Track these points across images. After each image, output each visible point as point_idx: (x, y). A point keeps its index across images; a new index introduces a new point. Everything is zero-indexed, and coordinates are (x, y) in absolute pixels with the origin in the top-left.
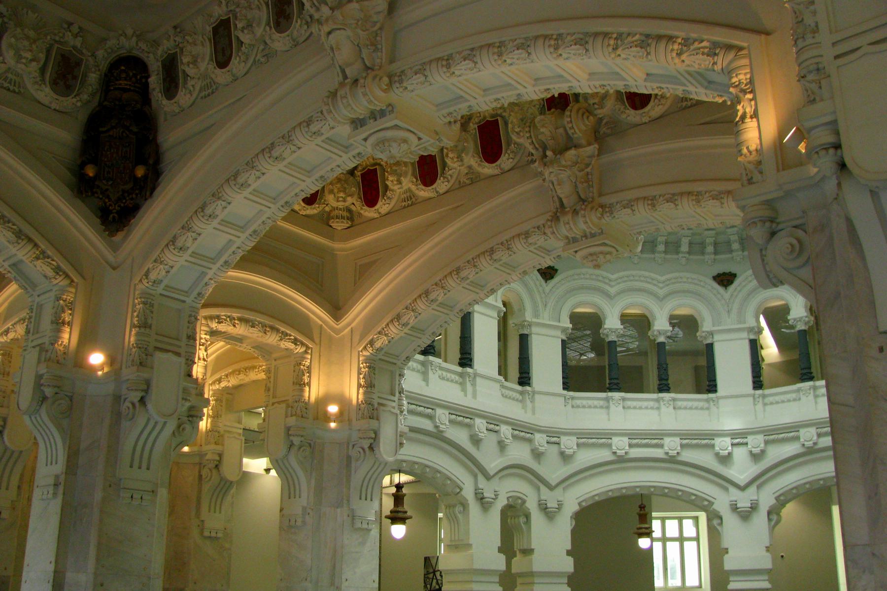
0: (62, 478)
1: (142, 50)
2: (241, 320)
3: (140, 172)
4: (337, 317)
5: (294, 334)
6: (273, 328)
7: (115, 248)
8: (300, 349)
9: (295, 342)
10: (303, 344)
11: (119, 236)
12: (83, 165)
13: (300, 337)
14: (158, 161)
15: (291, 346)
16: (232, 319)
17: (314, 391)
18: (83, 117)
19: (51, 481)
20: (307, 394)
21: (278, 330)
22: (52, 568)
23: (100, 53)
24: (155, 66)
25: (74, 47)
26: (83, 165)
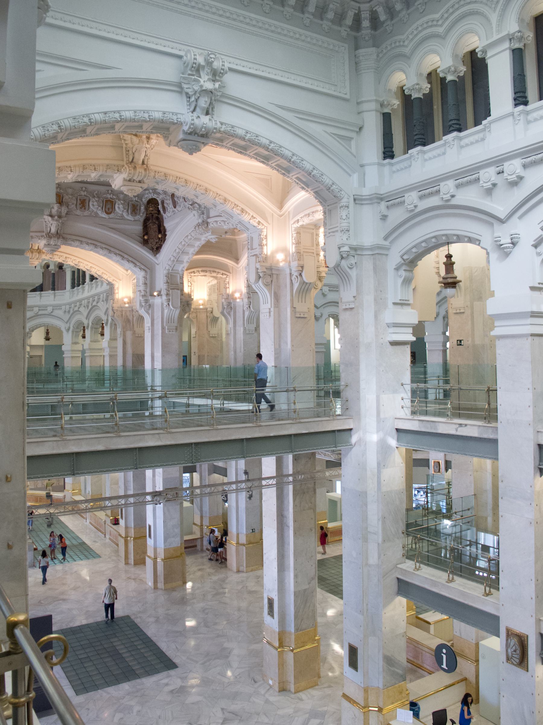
0: (150, 328)
1: (155, 196)
2: (202, 271)
3: (160, 236)
4: (237, 263)
5: (222, 272)
6: (214, 272)
7: (157, 259)
8: (225, 276)
9: (223, 274)
10: (225, 274)
11: (158, 256)
12: (144, 236)
13: (224, 272)
14: (165, 231)
15: (221, 276)
16: (198, 271)
17: (230, 291)
18: (142, 220)
19: (148, 328)
20: (228, 291)
21: (215, 272)
22: (150, 352)
23: (143, 200)
24: (160, 202)
25: (136, 201)
26: (144, 236)
